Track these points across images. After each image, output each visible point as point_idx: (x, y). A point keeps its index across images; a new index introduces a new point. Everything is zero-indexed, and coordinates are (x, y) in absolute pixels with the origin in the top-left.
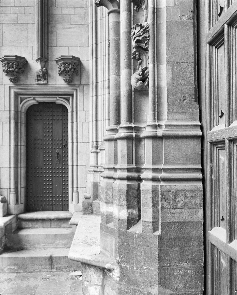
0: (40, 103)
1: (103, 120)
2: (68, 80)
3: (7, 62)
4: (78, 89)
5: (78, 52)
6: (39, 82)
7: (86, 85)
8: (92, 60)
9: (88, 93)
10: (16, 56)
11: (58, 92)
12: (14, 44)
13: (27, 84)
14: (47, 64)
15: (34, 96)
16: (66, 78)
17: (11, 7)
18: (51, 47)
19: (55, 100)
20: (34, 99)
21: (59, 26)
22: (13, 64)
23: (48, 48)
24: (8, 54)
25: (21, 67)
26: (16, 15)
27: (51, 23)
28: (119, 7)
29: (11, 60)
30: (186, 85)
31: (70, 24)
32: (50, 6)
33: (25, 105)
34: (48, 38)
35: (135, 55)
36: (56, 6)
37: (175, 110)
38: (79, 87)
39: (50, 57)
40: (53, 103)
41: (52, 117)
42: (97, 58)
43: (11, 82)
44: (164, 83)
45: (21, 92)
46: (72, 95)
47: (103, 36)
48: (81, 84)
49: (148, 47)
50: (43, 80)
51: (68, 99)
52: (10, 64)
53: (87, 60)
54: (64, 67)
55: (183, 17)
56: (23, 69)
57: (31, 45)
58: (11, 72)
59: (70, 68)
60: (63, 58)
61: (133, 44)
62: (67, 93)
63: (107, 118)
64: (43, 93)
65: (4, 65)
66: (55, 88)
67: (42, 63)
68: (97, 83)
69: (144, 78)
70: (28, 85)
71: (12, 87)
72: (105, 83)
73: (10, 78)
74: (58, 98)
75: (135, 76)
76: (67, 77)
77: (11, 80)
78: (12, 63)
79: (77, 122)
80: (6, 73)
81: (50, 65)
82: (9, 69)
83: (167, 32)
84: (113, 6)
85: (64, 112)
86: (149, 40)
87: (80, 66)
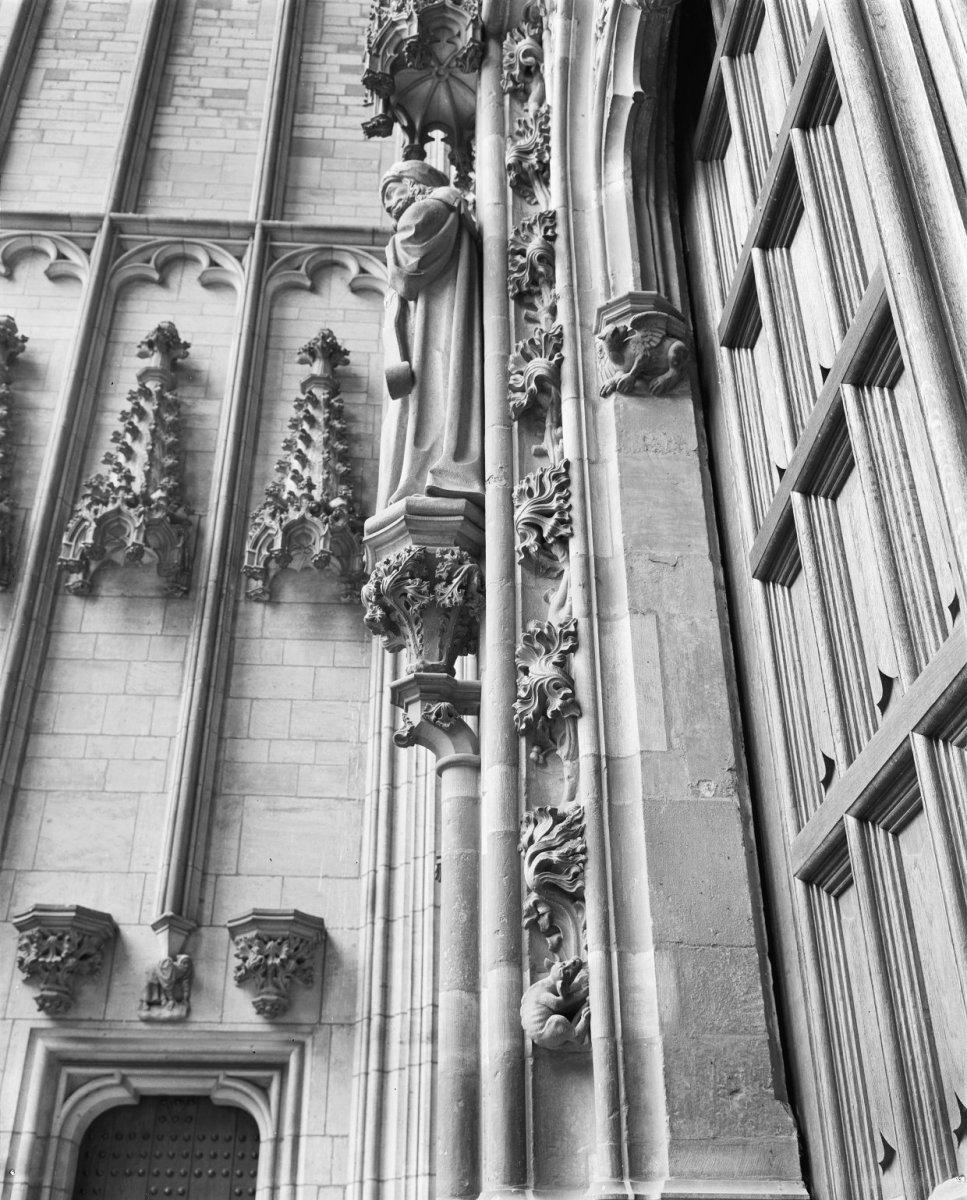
0: (145, 1100)
1: (407, 1177)
2: (272, 1006)
3: (39, 931)
4: (309, 1041)
5: (320, 895)
6: (156, 1012)
7: (342, 1025)
8: (369, 926)
9: (349, 1061)
10: (79, 910)
11: (227, 1053)
12: (77, 864)
13: (103, 1020)
14: (192, 939)
15: (125, 1071)
16: (264, 997)
17: (87, 735)
18: (217, 876)
19: (210, 1089)
20: (124, 1082)
21: (253, 803)
22: (61, 939)
23: (203, 881)
24: (46, 900)
25: (93, 951)
26: (104, 763)
27: (227, 791)
28: (477, 750)
29: (55, 923)
30: (734, 1031)
31: (296, 796)
32: (227, 734)
33: (83, 1110)
34: (208, 845)
35: (535, 916)
36: (252, 735)
37: (698, 1134)
38: (311, 1033)
39: (207, 912)
40: (202, 1101)
41: (187, 1162)
42: (388, 921)
43: (39, 1010)
44: (650, 1025)
45: (75, 1052)
46: (282, 1068)
47: (416, 841)
48: (320, 1023)
49: (582, 889)
50: (171, 1003)
51: (263, 1084)
52: (51, 938)
53: (352, 929)
54: (259, 952)
55: (703, 787)
56: (98, 957)
57: (144, 869)
58: (46, 970)
59: (283, 956)
60: (258, 919)
61: (529, 875)
62: (262, 1058)
63: (424, 1167)
64: (162, 1057)
65: (25, 941)
66: (214, 1037)
67: (175, 935)
68: (385, 1016)
69: (571, 1004)
70: (107, 1025)
71: (42, 1029)
72: (417, 1019)
73: (38, 994)
74: (222, 1081)
75: (538, 995)
76: (268, 993)
77: (43, 1003)
78: (60, 934)
79: (294, 1185)
80: (29, 972)
81: (204, 945)
82: (41, 959)
83: (649, 838)
84: (455, 746)
85: (243, 1139)
86: (584, 862)
87: (321, 949)
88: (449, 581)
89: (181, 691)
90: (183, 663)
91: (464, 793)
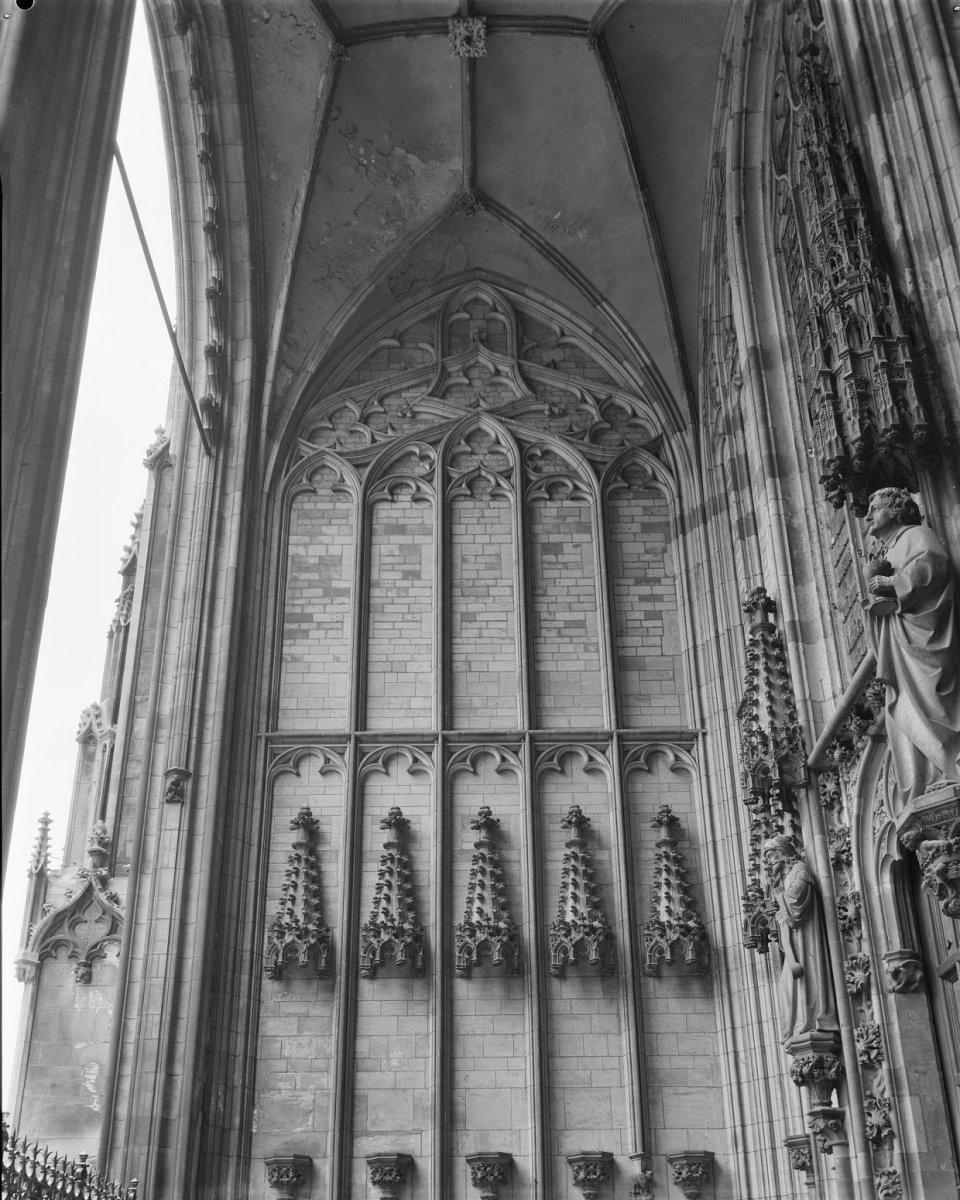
21: (666, 1090)
28: (846, 1137)
39: (653, 1148)
86: (901, 1194)
88: (830, 1069)
89: (620, 1030)
90: (618, 1015)
91: (843, 1156)
